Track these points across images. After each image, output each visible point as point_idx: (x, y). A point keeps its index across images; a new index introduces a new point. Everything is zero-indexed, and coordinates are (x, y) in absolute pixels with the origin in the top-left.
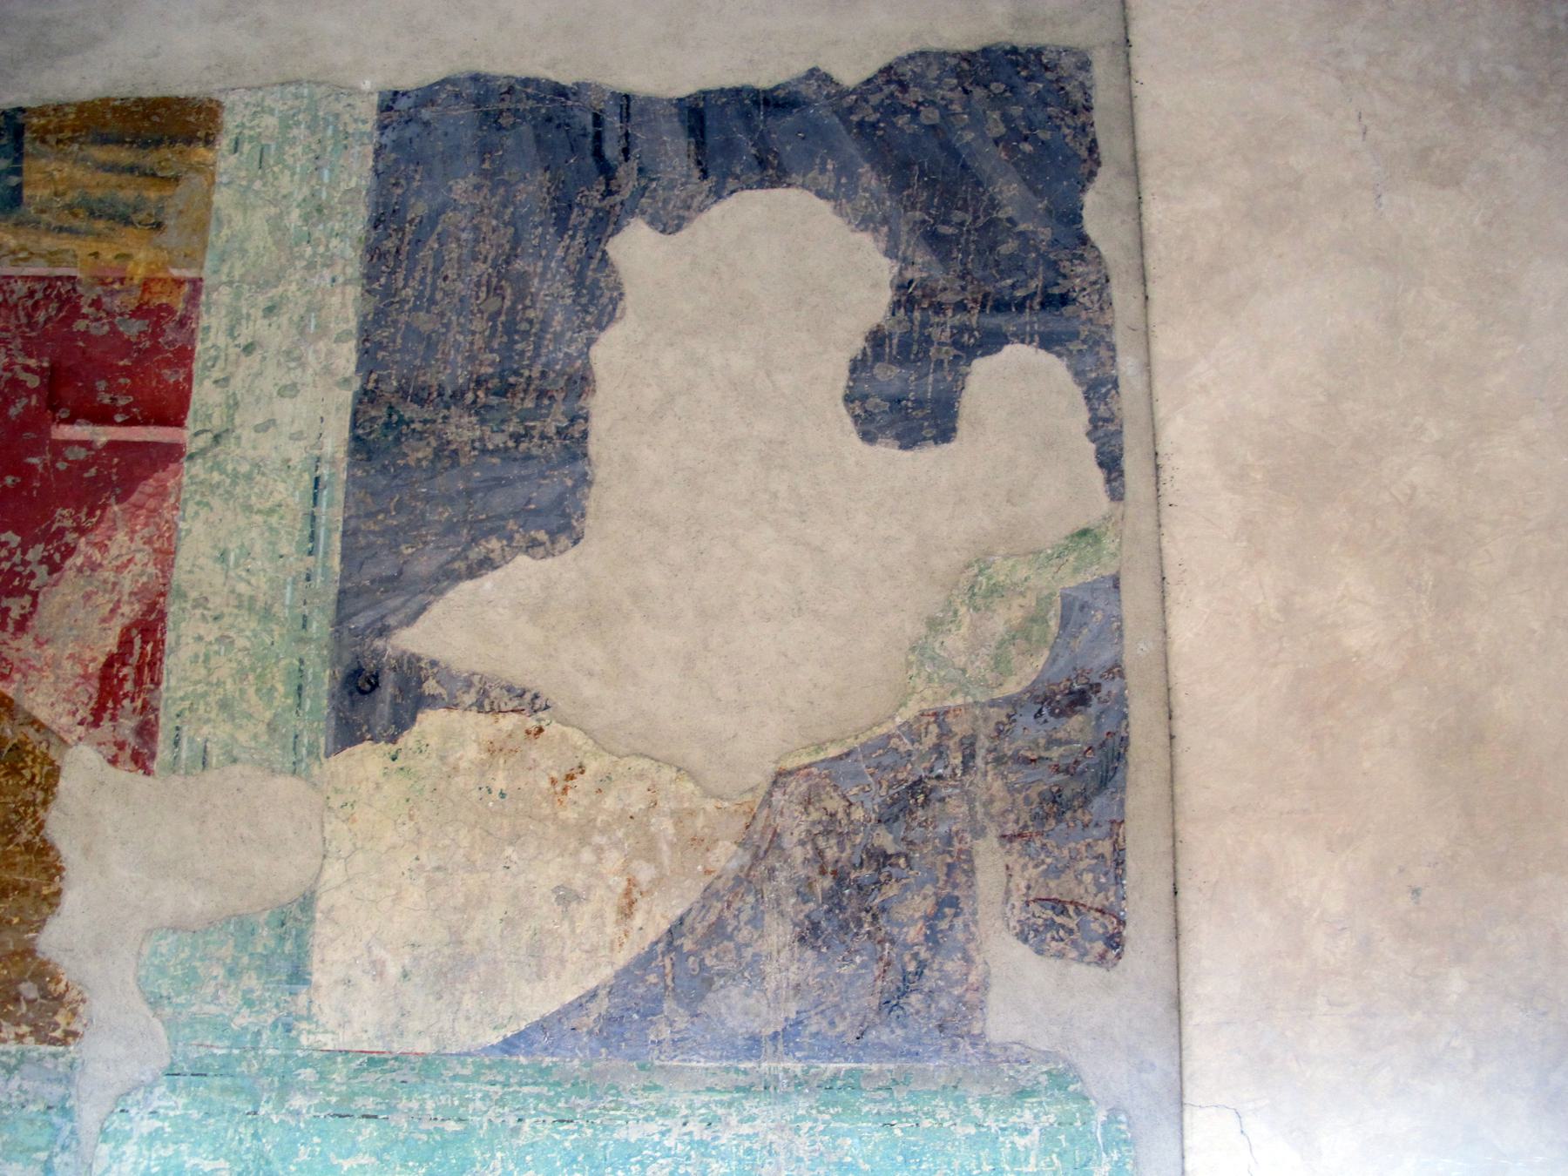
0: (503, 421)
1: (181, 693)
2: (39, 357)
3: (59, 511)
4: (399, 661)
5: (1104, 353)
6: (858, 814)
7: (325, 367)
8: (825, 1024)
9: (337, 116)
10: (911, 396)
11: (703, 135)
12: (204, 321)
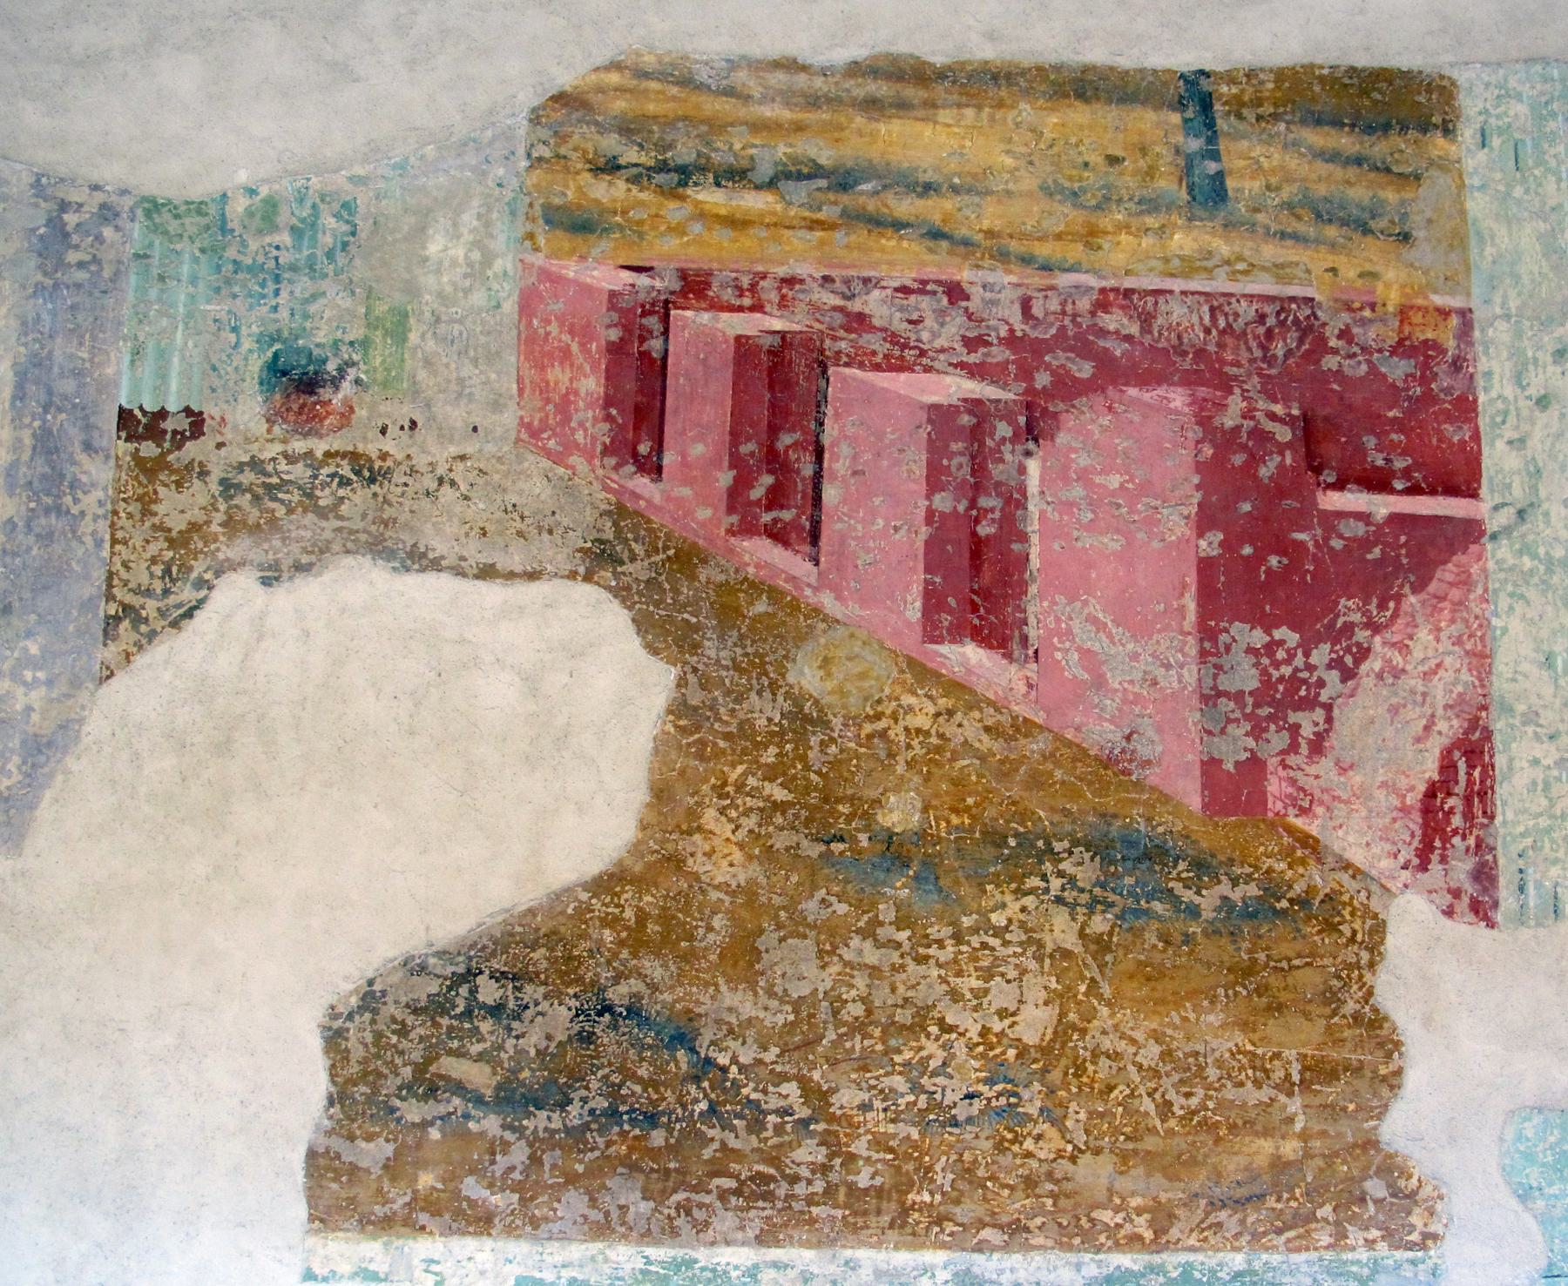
1: (1521, 829)
2: (1286, 401)
3: (1343, 601)
12: (1483, 364)
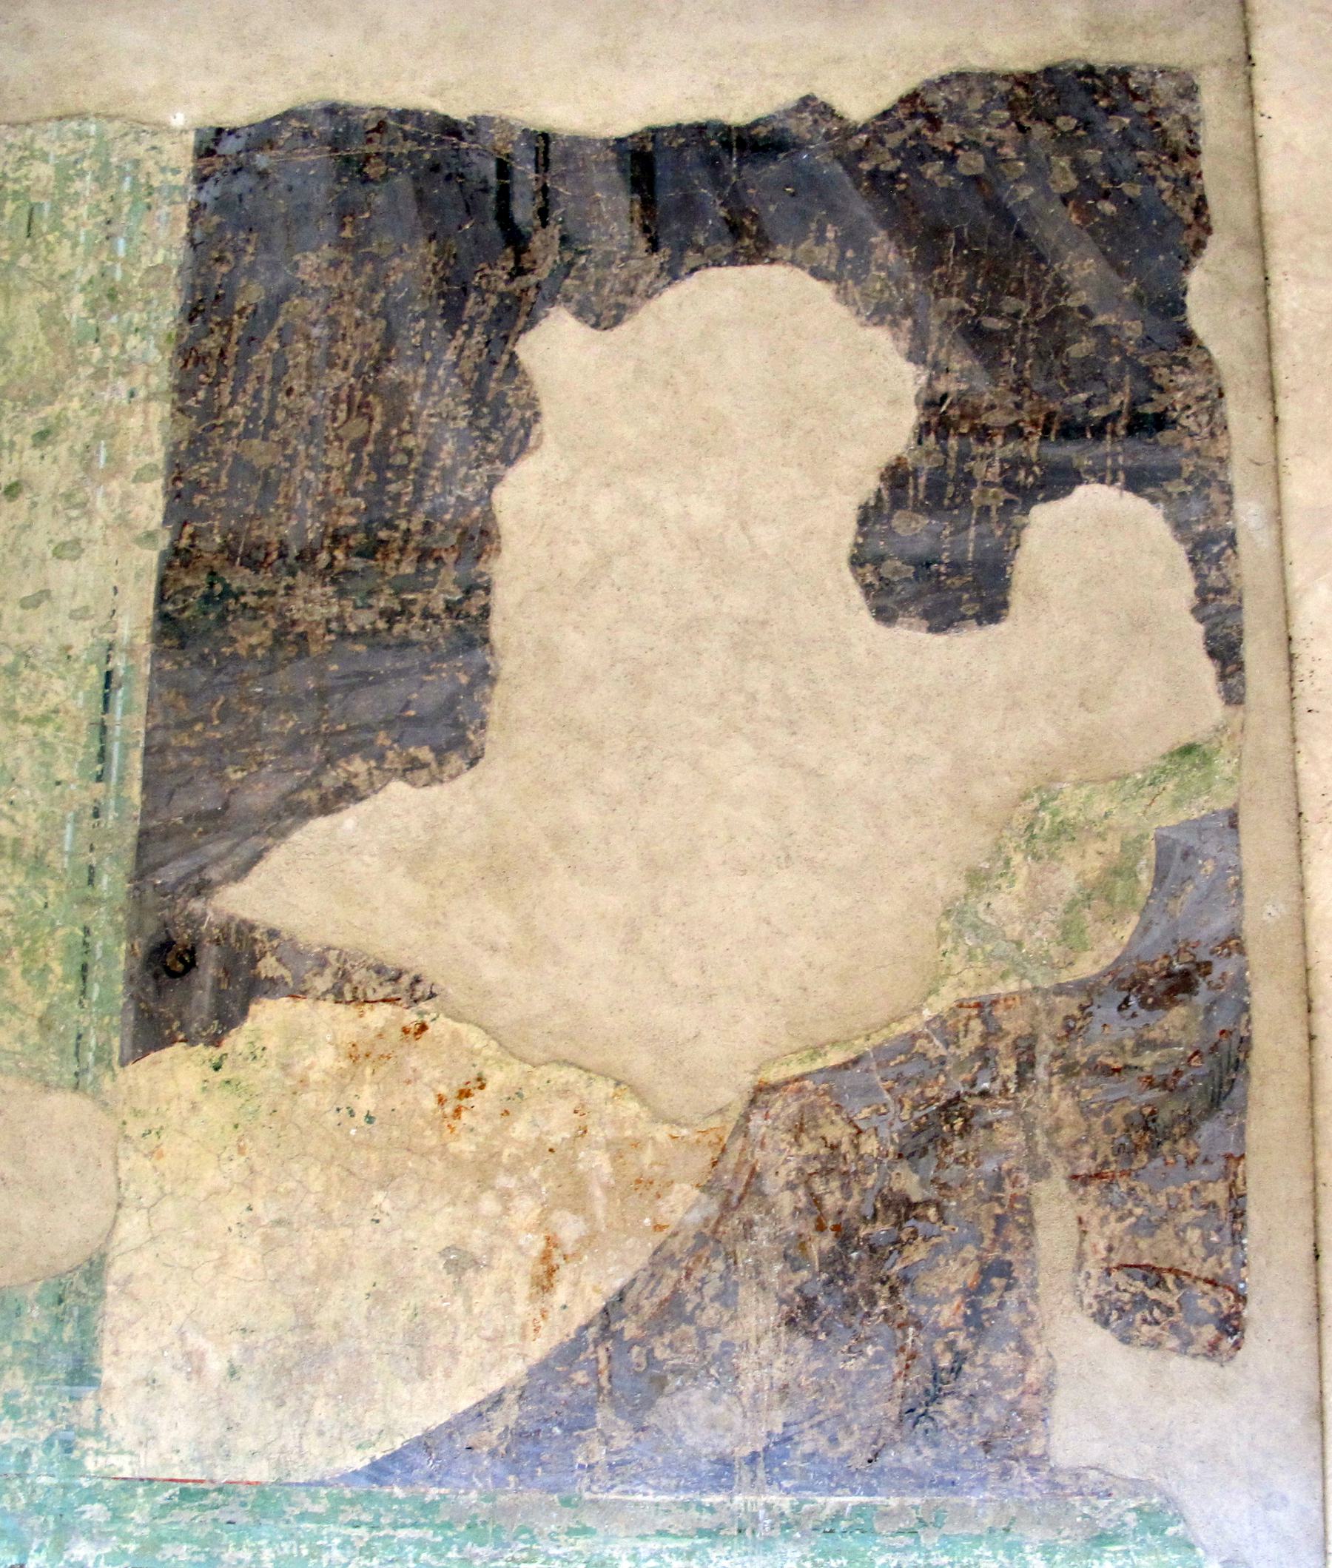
0: (371, 593)
4: (224, 929)
5: (1216, 497)
6: (870, 1146)
7: (120, 517)
8: (823, 1441)
9: (137, 163)
10: (945, 557)
11: (652, 190)
